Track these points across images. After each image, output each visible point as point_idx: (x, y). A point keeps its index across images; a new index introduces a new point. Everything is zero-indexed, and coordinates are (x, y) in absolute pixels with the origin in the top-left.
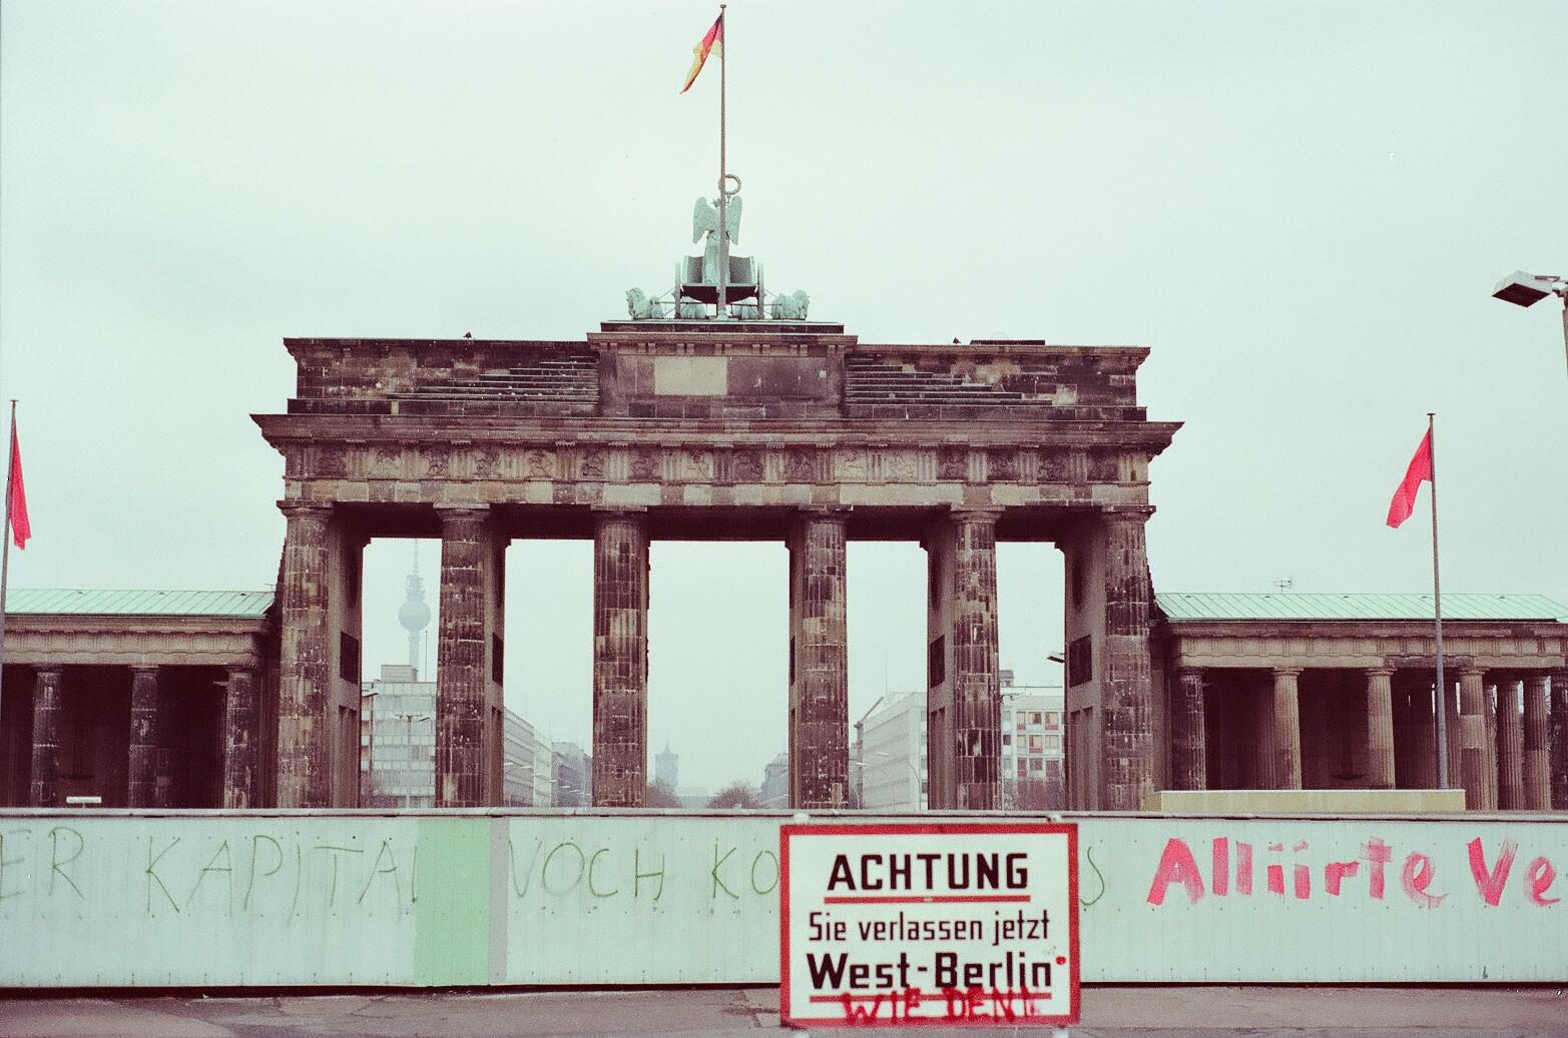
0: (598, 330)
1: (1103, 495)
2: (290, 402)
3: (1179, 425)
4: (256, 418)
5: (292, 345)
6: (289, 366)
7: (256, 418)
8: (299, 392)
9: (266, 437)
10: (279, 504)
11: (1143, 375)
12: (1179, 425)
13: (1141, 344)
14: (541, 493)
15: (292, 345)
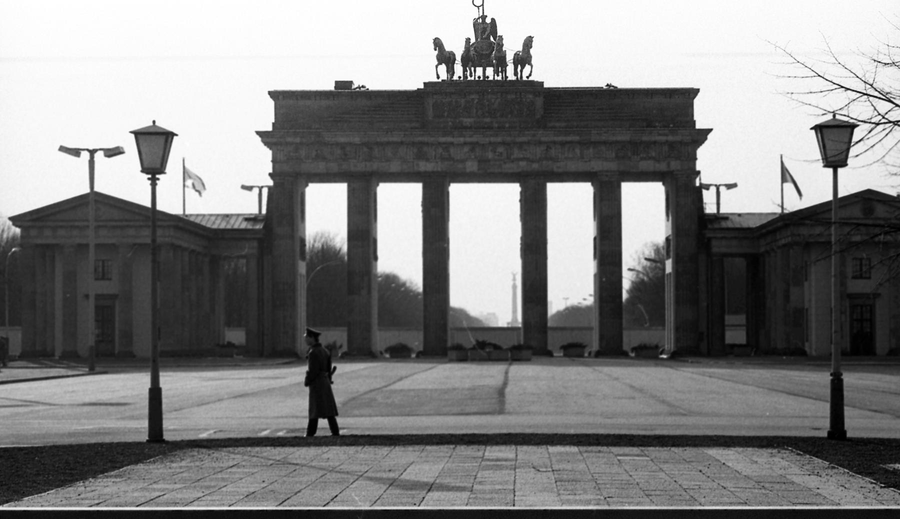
0: (422, 87)
1: (675, 165)
2: (273, 124)
3: (710, 130)
4: (258, 133)
5: (273, 95)
6: (271, 103)
7: (258, 133)
8: (276, 118)
9: (263, 141)
10: (270, 174)
11: (698, 103)
12: (710, 130)
13: (696, 87)
14: (395, 167)
15: (273, 95)
